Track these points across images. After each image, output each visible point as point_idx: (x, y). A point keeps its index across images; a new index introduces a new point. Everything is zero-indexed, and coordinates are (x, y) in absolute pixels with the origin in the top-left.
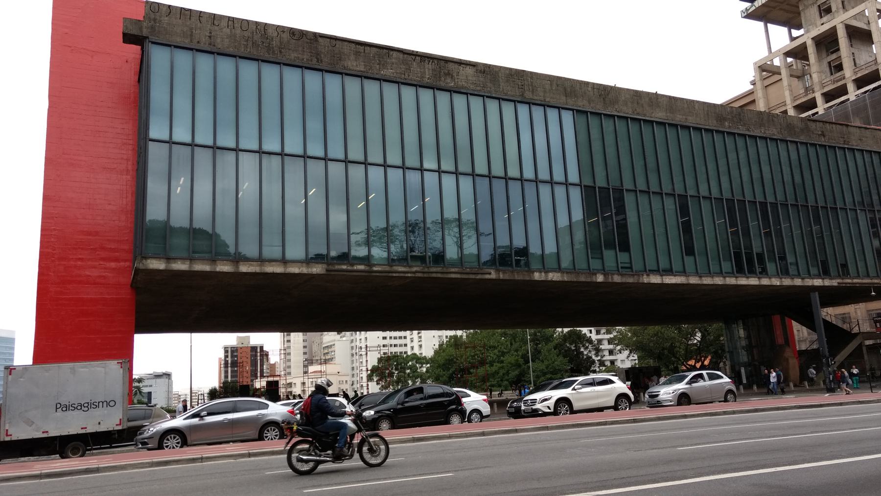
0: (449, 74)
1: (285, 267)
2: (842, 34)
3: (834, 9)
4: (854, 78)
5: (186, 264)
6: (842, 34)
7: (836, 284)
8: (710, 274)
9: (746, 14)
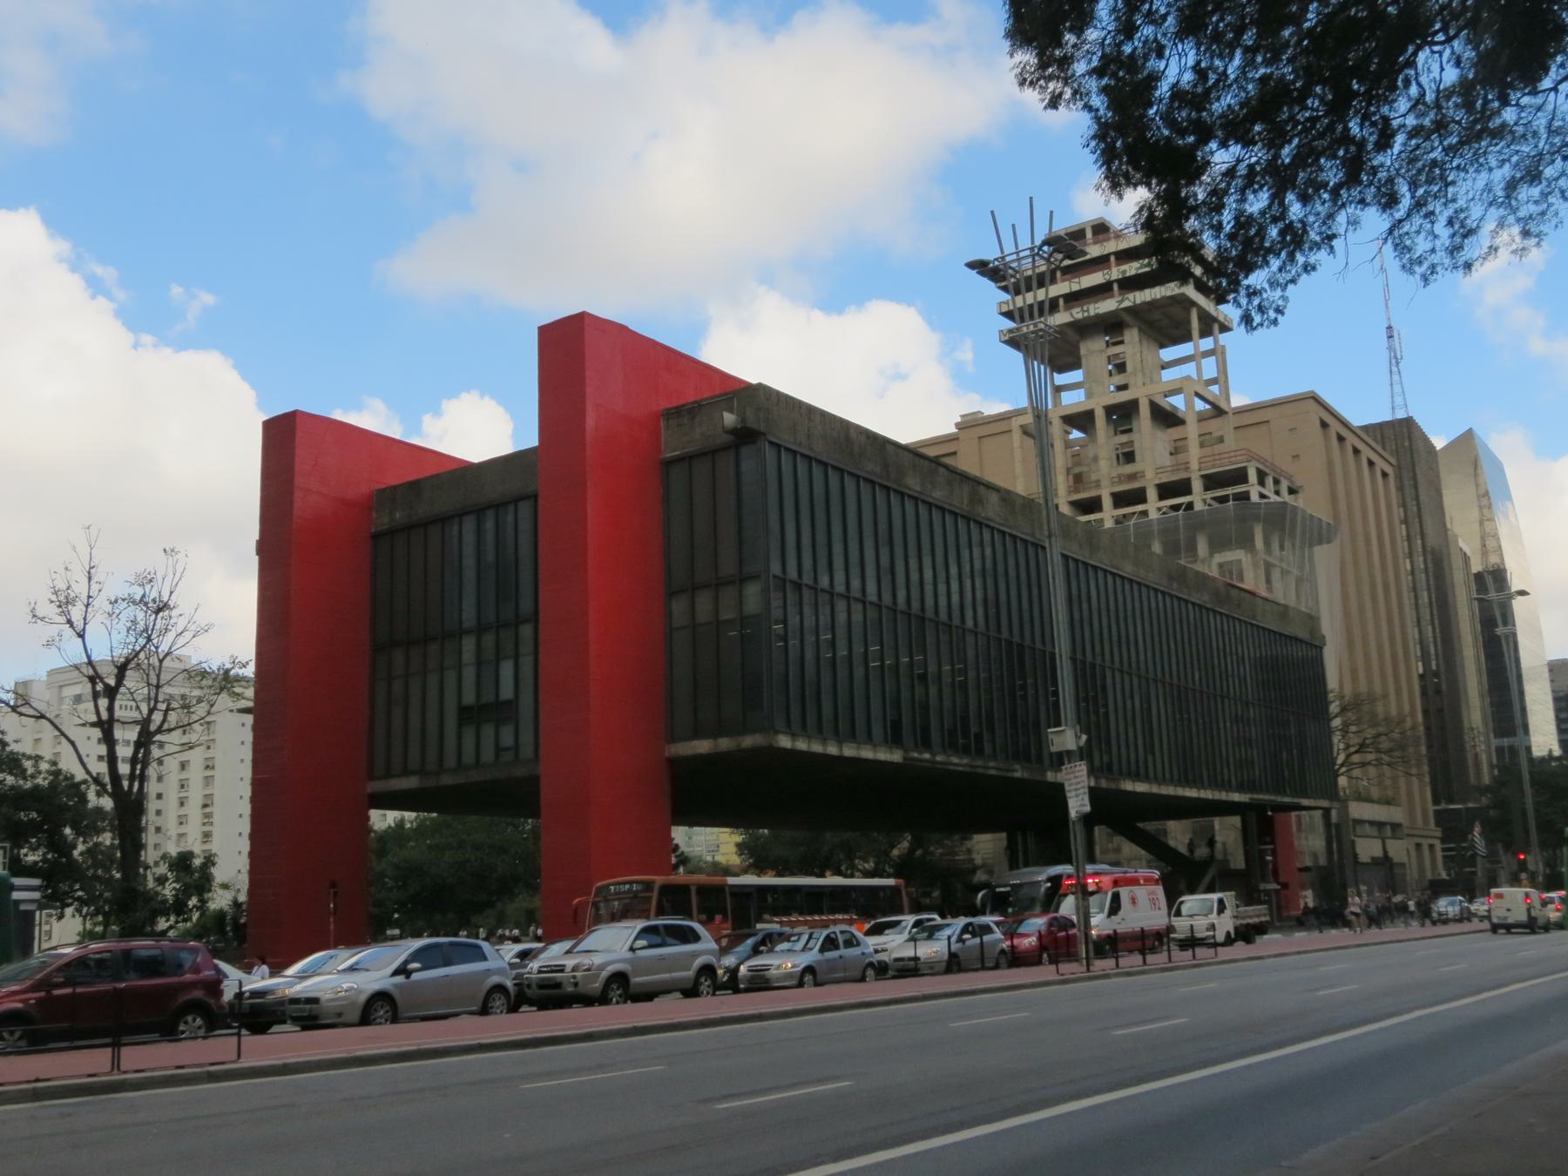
0: (981, 501)
1: (875, 751)
2: (1144, 409)
3: (1129, 368)
4: (1157, 482)
6: (1144, 409)
7: (1247, 800)
8: (852, 737)
9: (1007, 338)
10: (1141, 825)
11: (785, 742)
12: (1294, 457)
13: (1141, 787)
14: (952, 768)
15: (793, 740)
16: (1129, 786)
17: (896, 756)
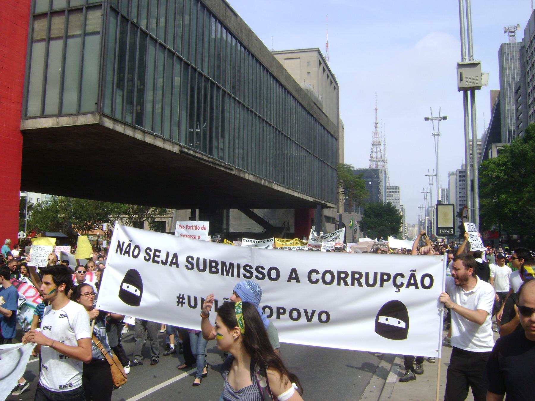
5: (121, 127)
7: (313, 201)
10: (252, 210)
11: (108, 124)
12: (308, 73)
13: (280, 189)
14: (203, 162)
15: (114, 124)
16: (276, 187)
17: (176, 149)
